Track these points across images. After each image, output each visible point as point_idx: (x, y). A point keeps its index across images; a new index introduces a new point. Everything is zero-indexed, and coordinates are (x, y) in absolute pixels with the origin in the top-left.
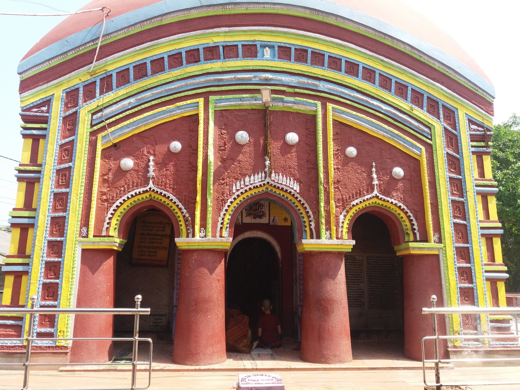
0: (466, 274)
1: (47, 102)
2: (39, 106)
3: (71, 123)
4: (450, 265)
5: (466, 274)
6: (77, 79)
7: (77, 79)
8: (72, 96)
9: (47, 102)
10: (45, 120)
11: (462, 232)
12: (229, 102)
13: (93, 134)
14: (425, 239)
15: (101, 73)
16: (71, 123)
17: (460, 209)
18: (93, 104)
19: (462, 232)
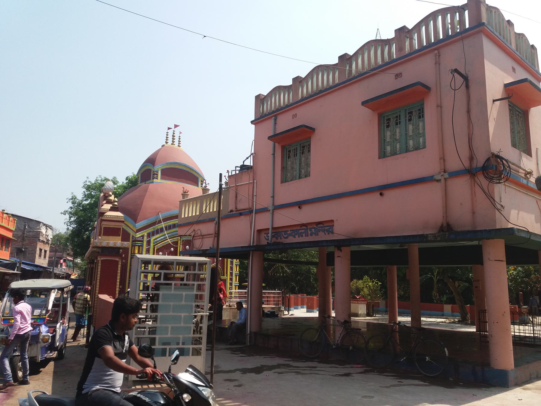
0: (231, 284)
1: (143, 236)
2: (140, 237)
3: (149, 243)
4: (228, 281)
5: (231, 284)
6: (150, 230)
7: (150, 230)
8: (149, 235)
9: (143, 236)
10: (142, 241)
11: (231, 274)
12: (184, 238)
13: (154, 246)
14: (224, 276)
15: (156, 229)
16: (149, 243)
17: (232, 268)
18: (154, 238)
19: (231, 274)
